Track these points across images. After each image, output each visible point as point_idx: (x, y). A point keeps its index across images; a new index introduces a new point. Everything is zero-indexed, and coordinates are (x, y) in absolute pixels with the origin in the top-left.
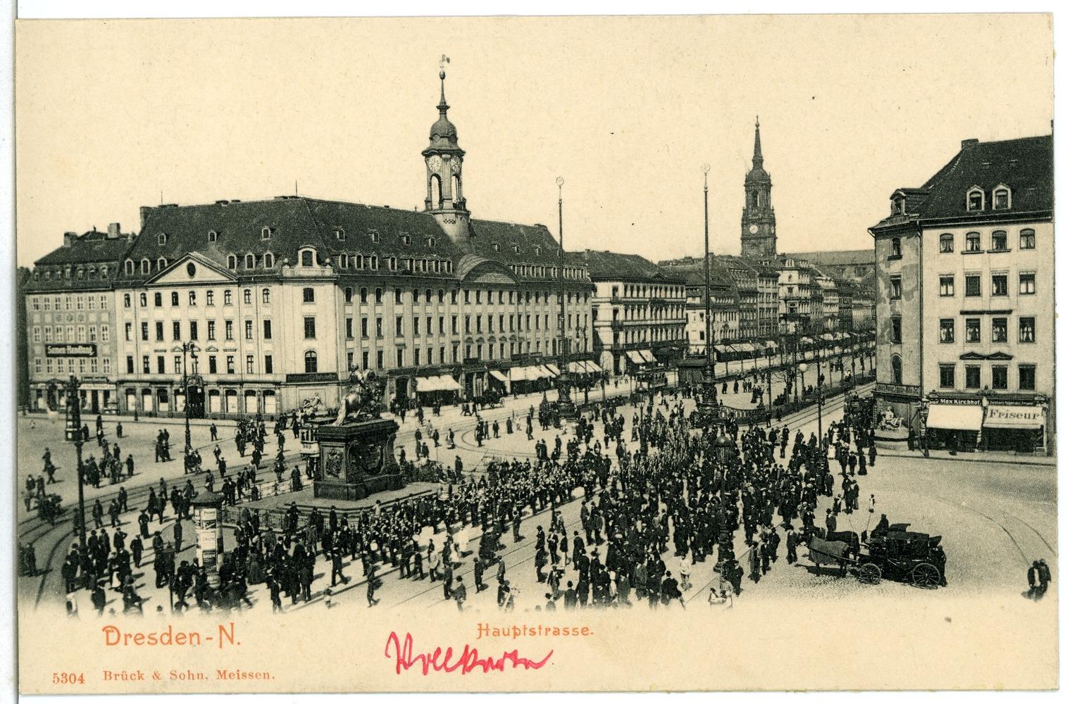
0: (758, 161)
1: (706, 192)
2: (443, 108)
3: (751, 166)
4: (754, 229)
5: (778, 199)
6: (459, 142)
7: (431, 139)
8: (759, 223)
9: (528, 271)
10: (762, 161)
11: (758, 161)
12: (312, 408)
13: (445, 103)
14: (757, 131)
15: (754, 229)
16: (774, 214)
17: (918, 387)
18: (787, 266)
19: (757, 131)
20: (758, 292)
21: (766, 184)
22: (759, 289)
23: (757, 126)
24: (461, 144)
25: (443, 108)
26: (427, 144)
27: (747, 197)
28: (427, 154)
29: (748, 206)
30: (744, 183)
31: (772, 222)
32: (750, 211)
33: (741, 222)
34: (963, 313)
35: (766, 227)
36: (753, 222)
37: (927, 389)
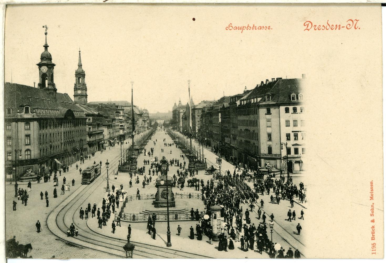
0: (80, 66)
1: (189, 90)
2: (46, 47)
3: (77, 67)
4: (79, 92)
5: (87, 80)
6: (52, 60)
7: (41, 59)
8: (82, 89)
9: (52, 112)
10: (81, 65)
11: (80, 66)
12: (29, 175)
13: (47, 45)
14: (80, 54)
15: (79, 92)
16: (86, 86)
17: (279, 155)
18: (119, 108)
19: (80, 54)
20: (115, 119)
21: (83, 75)
22: (116, 118)
23: (80, 52)
24: (53, 61)
25: (46, 47)
26: (39, 61)
27: (76, 79)
28: (40, 65)
29: (76, 82)
30: (75, 74)
31: (86, 90)
32: (77, 85)
33: (74, 89)
34: (293, 132)
35: (84, 91)
36: (79, 89)
37: (283, 155)
